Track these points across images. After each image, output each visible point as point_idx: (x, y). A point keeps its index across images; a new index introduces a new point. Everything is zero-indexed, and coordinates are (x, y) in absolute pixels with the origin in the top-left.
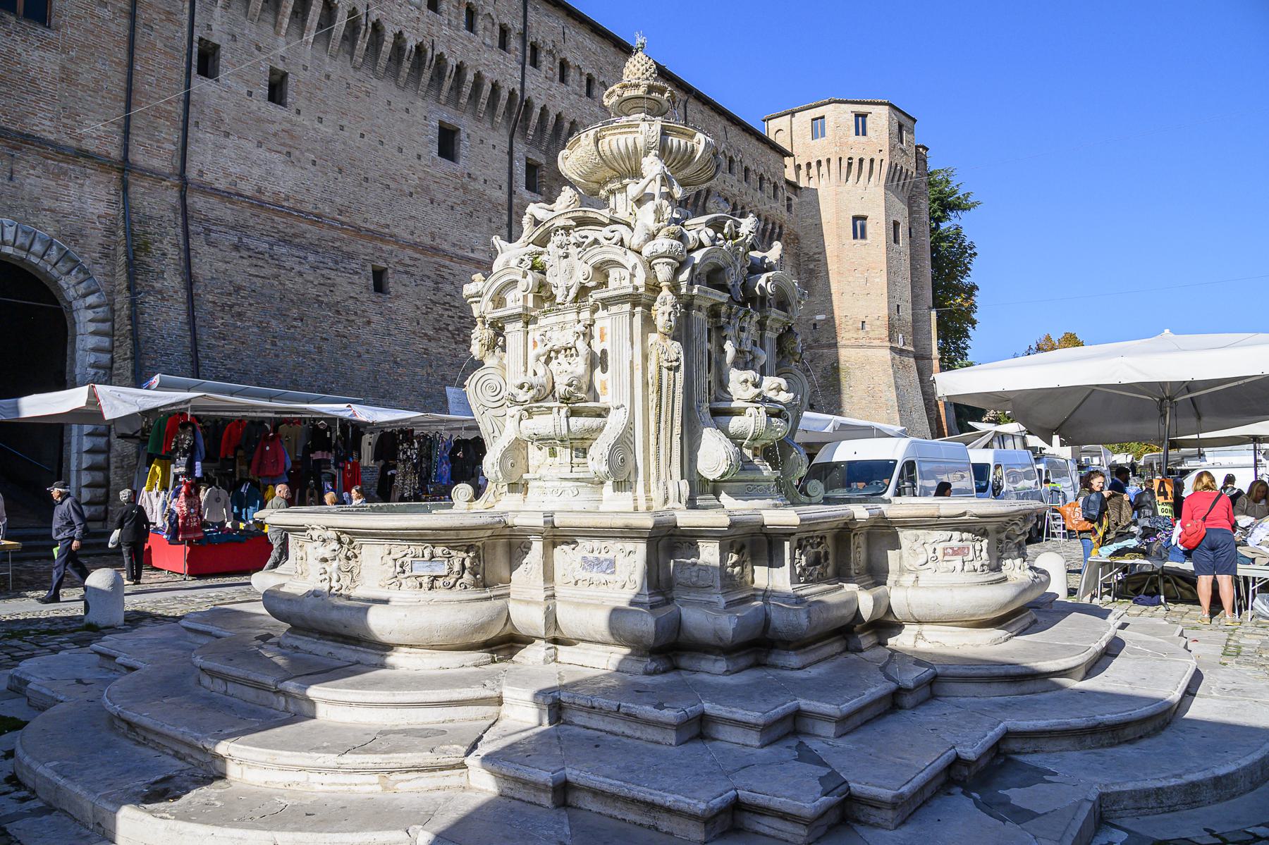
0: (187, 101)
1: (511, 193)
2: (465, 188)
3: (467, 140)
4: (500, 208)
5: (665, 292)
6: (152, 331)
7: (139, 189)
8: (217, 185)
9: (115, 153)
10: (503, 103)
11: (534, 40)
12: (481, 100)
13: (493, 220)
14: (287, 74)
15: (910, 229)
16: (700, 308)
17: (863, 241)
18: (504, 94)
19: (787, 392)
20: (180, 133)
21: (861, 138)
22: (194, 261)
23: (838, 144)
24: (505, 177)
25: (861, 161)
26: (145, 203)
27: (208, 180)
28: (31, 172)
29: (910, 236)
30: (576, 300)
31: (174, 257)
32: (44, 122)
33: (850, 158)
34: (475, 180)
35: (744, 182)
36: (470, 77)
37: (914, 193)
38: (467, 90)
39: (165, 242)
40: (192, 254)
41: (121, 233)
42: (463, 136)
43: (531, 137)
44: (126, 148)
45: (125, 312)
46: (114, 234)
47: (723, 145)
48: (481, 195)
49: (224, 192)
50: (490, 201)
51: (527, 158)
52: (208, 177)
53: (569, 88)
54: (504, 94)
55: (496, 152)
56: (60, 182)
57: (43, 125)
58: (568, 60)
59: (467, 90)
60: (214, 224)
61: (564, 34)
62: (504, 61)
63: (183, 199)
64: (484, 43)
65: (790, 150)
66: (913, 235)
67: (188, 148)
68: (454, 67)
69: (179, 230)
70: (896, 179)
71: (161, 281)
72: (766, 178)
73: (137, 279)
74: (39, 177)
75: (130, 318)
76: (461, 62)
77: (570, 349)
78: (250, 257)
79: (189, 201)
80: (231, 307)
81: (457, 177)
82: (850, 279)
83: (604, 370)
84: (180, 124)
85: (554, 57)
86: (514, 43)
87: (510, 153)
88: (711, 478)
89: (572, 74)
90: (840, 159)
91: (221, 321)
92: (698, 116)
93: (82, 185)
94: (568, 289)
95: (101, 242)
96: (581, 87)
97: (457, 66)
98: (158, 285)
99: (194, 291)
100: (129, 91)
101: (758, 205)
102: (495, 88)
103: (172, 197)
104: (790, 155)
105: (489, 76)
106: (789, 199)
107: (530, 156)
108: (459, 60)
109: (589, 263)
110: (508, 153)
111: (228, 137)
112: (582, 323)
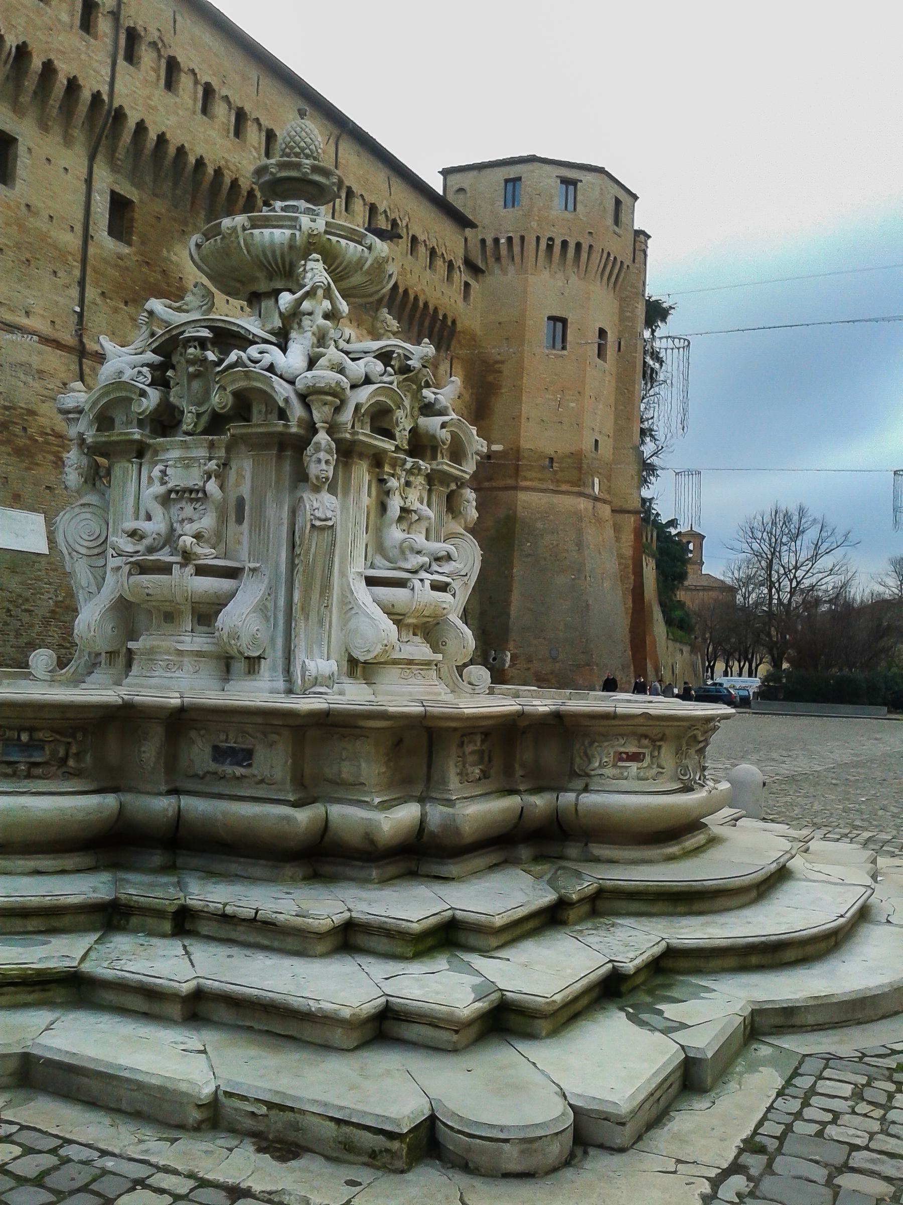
1: (87, 237)
2: (22, 227)
3: (28, 156)
4: (70, 258)
5: (322, 437)
10: (82, 109)
11: (132, 25)
12: (51, 102)
13: (59, 275)
17: (560, 353)
18: (86, 95)
21: (568, 215)
24: (80, 215)
25: (565, 244)
29: (619, 349)
33: (551, 239)
34: (36, 214)
35: (409, 256)
36: (37, 63)
38: (30, 83)
42: (22, 149)
43: (119, 163)
47: (385, 202)
48: (44, 237)
50: (56, 248)
51: (113, 193)
53: (177, 100)
54: (86, 95)
55: (69, 177)
58: (179, 59)
59: (30, 83)
61: (175, 22)
62: (88, 49)
64: (59, 20)
65: (471, 217)
68: (14, 50)
72: (439, 253)
76: (24, 43)
77: (197, 491)
81: (9, 207)
82: (539, 400)
83: (240, 520)
85: (158, 50)
86: (104, 25)
87: (89, 182)
88: (362, 659)
89: (185, 81)
90: (538, 238)
94: (199, 415)
96: (195, 100)
97: (18, 47)
101: (426, 290)
102: (73, 86)
104: (472, 225)
105: (64, 69)
106: (467, 285)
107: (117, 189)
108: (21, 40)
109: (229, 390)
110: (86, 180)
112: (214, 462)
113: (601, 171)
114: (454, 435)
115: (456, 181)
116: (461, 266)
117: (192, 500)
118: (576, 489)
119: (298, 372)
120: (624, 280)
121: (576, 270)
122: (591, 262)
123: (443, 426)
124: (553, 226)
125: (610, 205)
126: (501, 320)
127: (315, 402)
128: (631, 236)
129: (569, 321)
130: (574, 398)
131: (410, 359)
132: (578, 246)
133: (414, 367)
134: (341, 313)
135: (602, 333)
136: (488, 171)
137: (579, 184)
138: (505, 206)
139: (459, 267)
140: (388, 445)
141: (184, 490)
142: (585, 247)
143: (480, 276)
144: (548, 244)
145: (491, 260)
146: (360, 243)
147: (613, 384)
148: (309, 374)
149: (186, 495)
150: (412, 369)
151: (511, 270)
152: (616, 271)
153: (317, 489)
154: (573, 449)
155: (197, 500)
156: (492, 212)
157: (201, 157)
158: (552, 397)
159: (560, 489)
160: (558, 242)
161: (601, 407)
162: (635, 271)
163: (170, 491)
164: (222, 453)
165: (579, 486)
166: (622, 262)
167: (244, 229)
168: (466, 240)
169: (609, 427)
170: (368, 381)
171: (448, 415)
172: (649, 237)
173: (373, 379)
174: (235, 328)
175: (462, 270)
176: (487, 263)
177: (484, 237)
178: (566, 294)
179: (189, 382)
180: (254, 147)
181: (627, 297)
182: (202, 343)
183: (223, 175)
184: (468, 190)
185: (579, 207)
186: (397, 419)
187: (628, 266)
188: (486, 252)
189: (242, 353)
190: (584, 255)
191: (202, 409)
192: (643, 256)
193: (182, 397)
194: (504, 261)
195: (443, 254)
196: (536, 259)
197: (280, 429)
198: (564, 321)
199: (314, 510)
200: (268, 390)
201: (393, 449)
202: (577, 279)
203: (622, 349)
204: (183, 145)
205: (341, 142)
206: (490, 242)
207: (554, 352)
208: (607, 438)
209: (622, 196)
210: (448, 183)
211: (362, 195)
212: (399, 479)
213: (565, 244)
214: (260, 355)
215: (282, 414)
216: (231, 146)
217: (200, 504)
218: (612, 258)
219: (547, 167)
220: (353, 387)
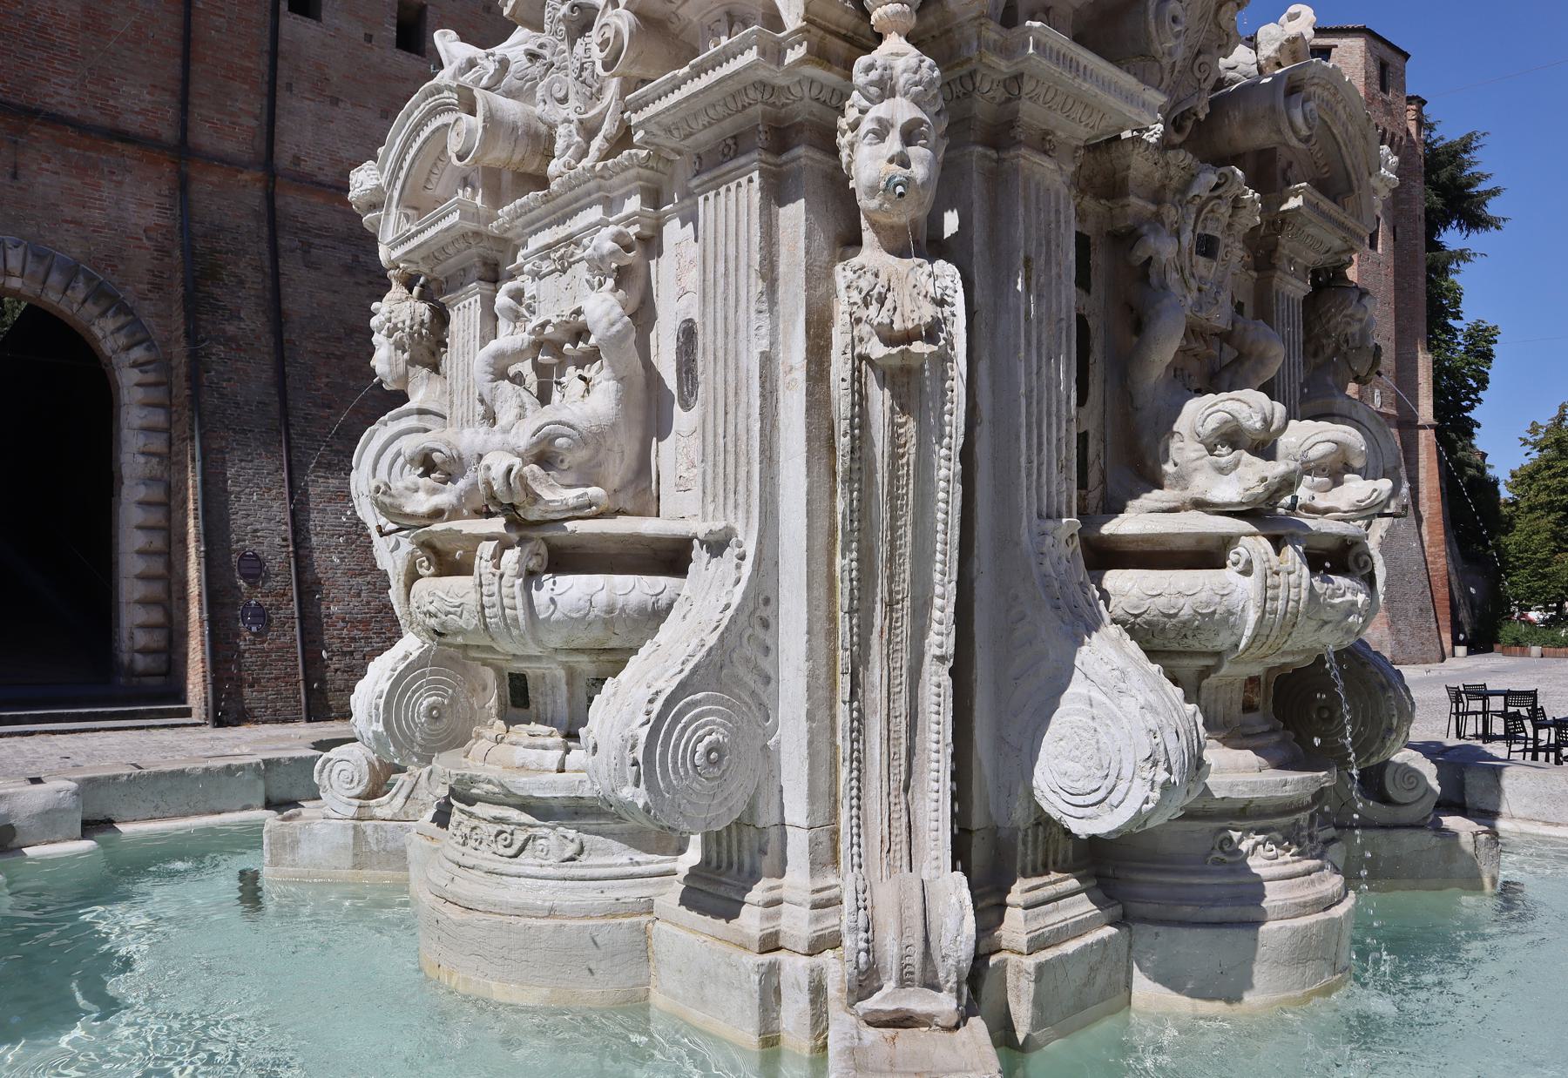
0: (274, 54)
6: (222, 396)
7: (206, 183)
8: (321, 178)
9: (168, 133)
14: (425, 7)
16: (1044, 143)
19: (1365, 474)
20: (265, 102)
22: (287, 291)
26: (214, 207)
27: (307, 169)
28: (45, 165)
31: (256, 286)
32: (61, 90)
39: (242, 265)
40: (283, 280)
41: (178, 253)
44: (184, 126)
45: (183, 370)
46: (168, 253)
49: (330, 187)
52: (308, 166)
56: (88, 180)
57: (60, 94)
60: (320, 236)
63: (270, 198)
67: (278, 123)
69: (264, 246)
71: (236, 323)
73: (201, 320)
74: (56, 173)
75: (189, 378)
78: (370, 283)
79: (279, 202)
80: (341, 358)
84: (265, 88)
91: (325, 380)
93: (120, 183)
95: (150, 267)
98: (230, 329)
99: (286, 336)
100: (187, 39)
103: (254, 197)
111: (337, 104)
172: (1424, 102)
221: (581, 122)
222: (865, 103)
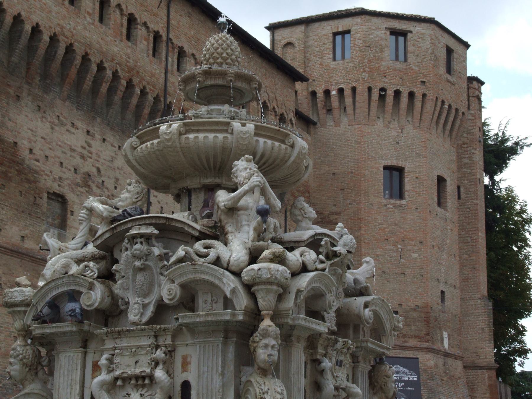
5: (267, 323)
15: (459, 188)
17: (398, 202)
21: (399, 65)
23: (367, 69)
25: (397, 94)
29: (459, 197)
30: (152, 321)
33: (383, 89)
37: (465, 140)
65: (301, 70)
66: (463, 196)
70: (442, 121)
72: (271, 108)
77: (144, 378)
82: (379, 251)
90: (370, 89)
92: (185, 21)
94: (145, 306)
104: (302, 78)
113: (431, 21)
114: (375, 313)
115: (283, 35)
116: (293, 119)
117: (136, 386)
118: (425, 345)
119: (242, 265)
120: (460, 127)
121: (410, 119)
122: (424, 111)
123: (366, 305)
124: (385, 76)
125: (442, 54)
126: (336, 171)
127: (260, 292)
128: (465, 85)
129: (406, 169)
130: (416, 248)
131: (335, 246)
132: (411, 95)
133: (340, 253)
134: (275, 208)
135: (441, 180)
136: (317, 25)
137: (409, 35)
138: (334, 59)
139: (291, 120)
140: (322, 328)
141: (130, 378)
142: (418, 97)
143: (312, 128)
144: (380, 96)
145: (322, 112)
146: (283, 142)
147: (456, 233)
148: (255, 266)
149: (133, 382)
150: (339, 255)
151: (345, 120)
152: (451, 119)
153: (264, 372)
154: (419, 302)
155: (143, 386)
156: (321, 64)
157: (37, 24)
158: (392, 247)
159: (406, 344)
160: (390, 93)
161: (445, 256)
162: (470, 117)
163: (116, 379)
164: (169, 342)
165: (428, 341)
166: (457, 110)
167: (180, 134)
168: (296, 92)
169: (455, 277)
170: (304, 269)
171: (368, 295)
172: (482, 83)
173: (310, 267)
174: (178, 225)
175: (294, 122)
176: (318, 114)
177: (314, 89)
178: (401, 143)
179: (135, 275)
180: (88, 13)
181: (464, 144)
182: (147, 238)
183: (58, 41)
184: (296, 45)
185: (411, 58)
186: (330, 303)
187: (463, 113)
188: (316, 104)
189: (189, 249)
190: (418, 104)
191: (147, 301)
192: (477, 101)
193: (128, 289)
194: (336, 112)
195: (274, 108)
196: (369, 111)
197: (228, 318)
198: (400, 170)
199: (263, 394)
200: (217, 282)
201: (326, 330)
202: (411, 128)
203: (462, 197)
204: (19, 15)
205: (172, 5)
206: (320, 94)
207: (393, 201)
208: (453, 289)
209: (452, 43)
210: (276, 38)
211: (193, 55)
212: (330, 359)
213: (397, 94)
214: (205, 250)
215: (228, 303)
216: (66, 13)
217: (145, 390)
218: (446, 106)
219: (375, 20)
220: (294, 275)
221: (143, 304)
222: (261, 338)
